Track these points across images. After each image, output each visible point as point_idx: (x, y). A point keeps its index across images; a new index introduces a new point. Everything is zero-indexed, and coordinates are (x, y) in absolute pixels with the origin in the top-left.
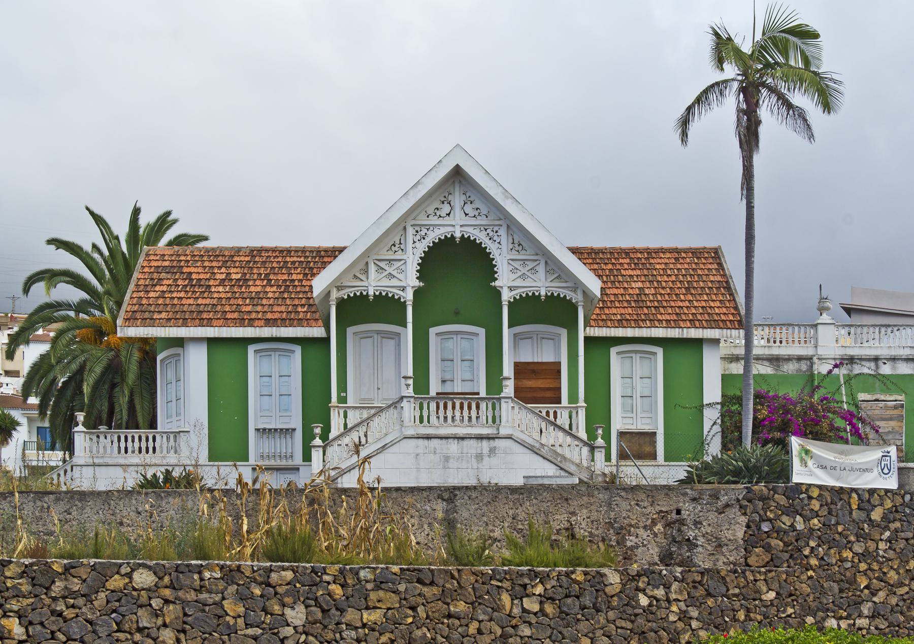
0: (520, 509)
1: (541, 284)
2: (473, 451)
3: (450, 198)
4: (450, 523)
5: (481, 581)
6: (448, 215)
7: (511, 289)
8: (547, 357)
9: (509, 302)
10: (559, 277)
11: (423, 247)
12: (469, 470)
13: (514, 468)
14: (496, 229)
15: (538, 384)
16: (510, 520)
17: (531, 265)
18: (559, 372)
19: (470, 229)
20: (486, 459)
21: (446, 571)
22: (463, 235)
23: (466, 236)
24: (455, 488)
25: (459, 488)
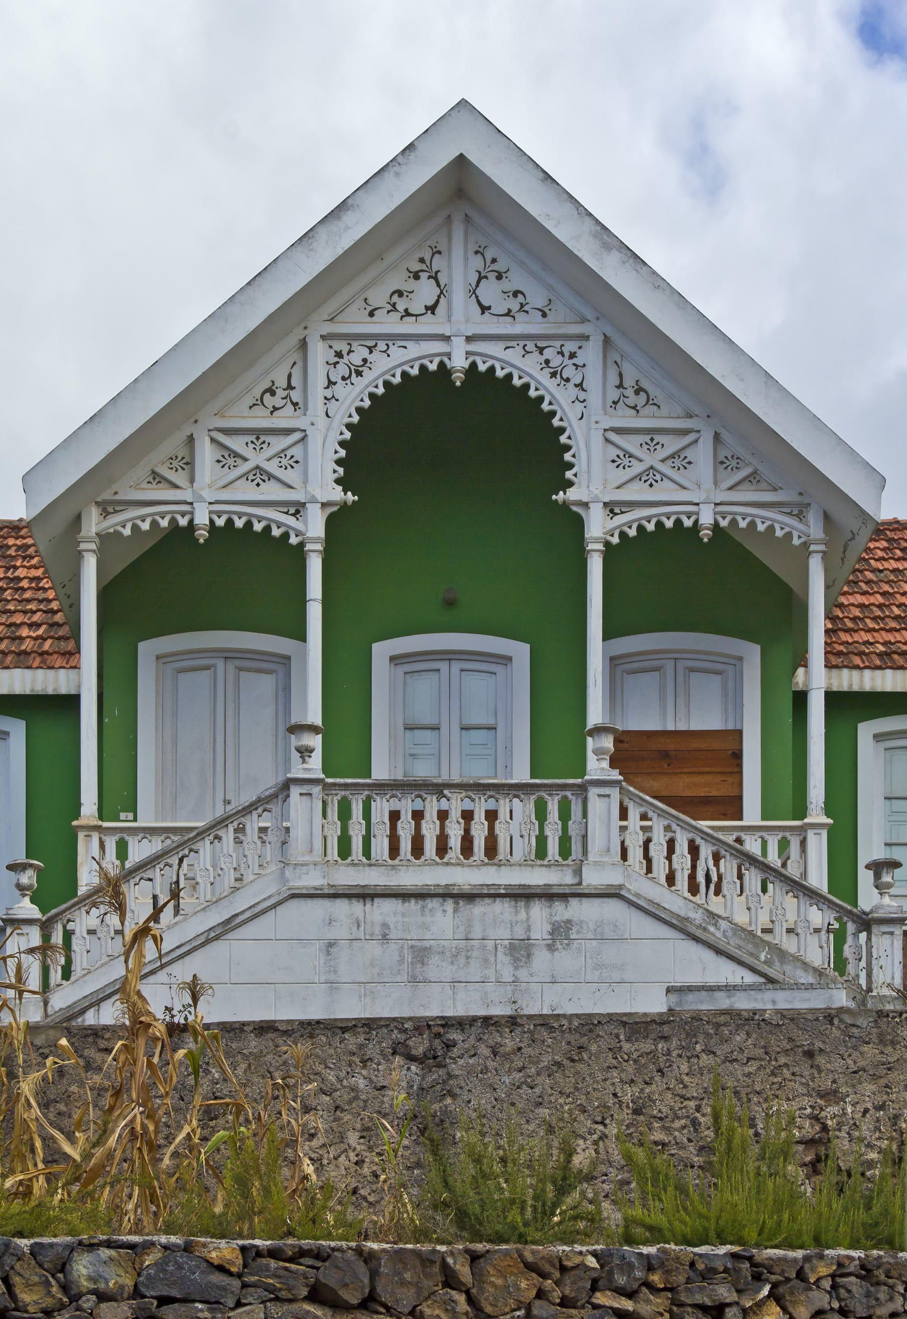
0: (659, 1084)
1: (701, 497)
2: (504, 933)
3: (438, 263)
4: (430, 1130)
5: (556, 1296)
6: (432, 309)
7: (612, 508)
8: (705, 718)
9: (607, 544)
10: (753, 478)
11: (353, 397)
12: (490, 987)
13: (634, 968)
14: (570, 346)
15: (683, 773)
16: (626, 1115)
17: (672, 444)
18: (738, 756)
19: (495, 349)
20: (541, 957)
21: (425, 1260)
22: (474, 365)
23: (482, 368)
24: (447, 1023)
25: (462, 1023)
